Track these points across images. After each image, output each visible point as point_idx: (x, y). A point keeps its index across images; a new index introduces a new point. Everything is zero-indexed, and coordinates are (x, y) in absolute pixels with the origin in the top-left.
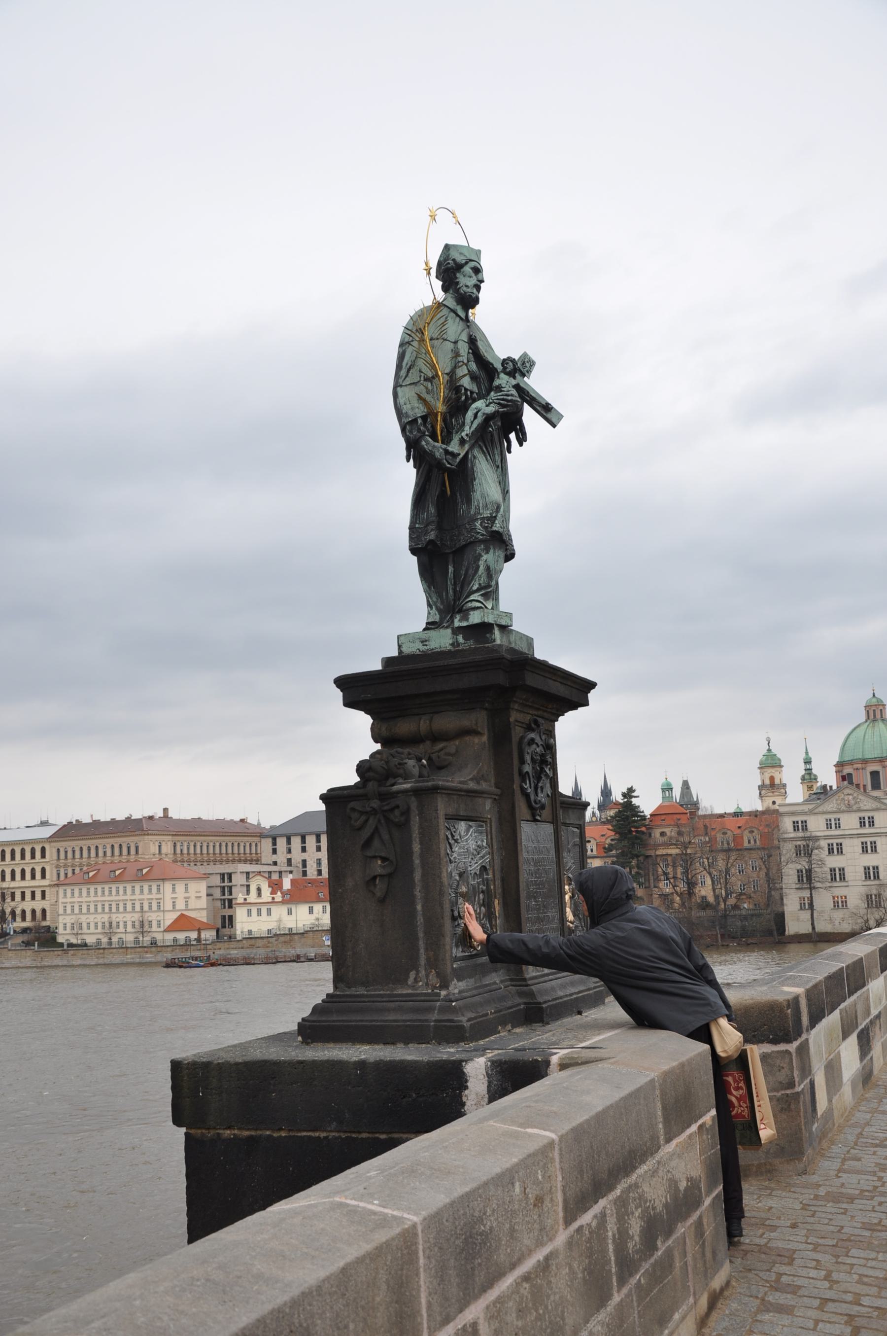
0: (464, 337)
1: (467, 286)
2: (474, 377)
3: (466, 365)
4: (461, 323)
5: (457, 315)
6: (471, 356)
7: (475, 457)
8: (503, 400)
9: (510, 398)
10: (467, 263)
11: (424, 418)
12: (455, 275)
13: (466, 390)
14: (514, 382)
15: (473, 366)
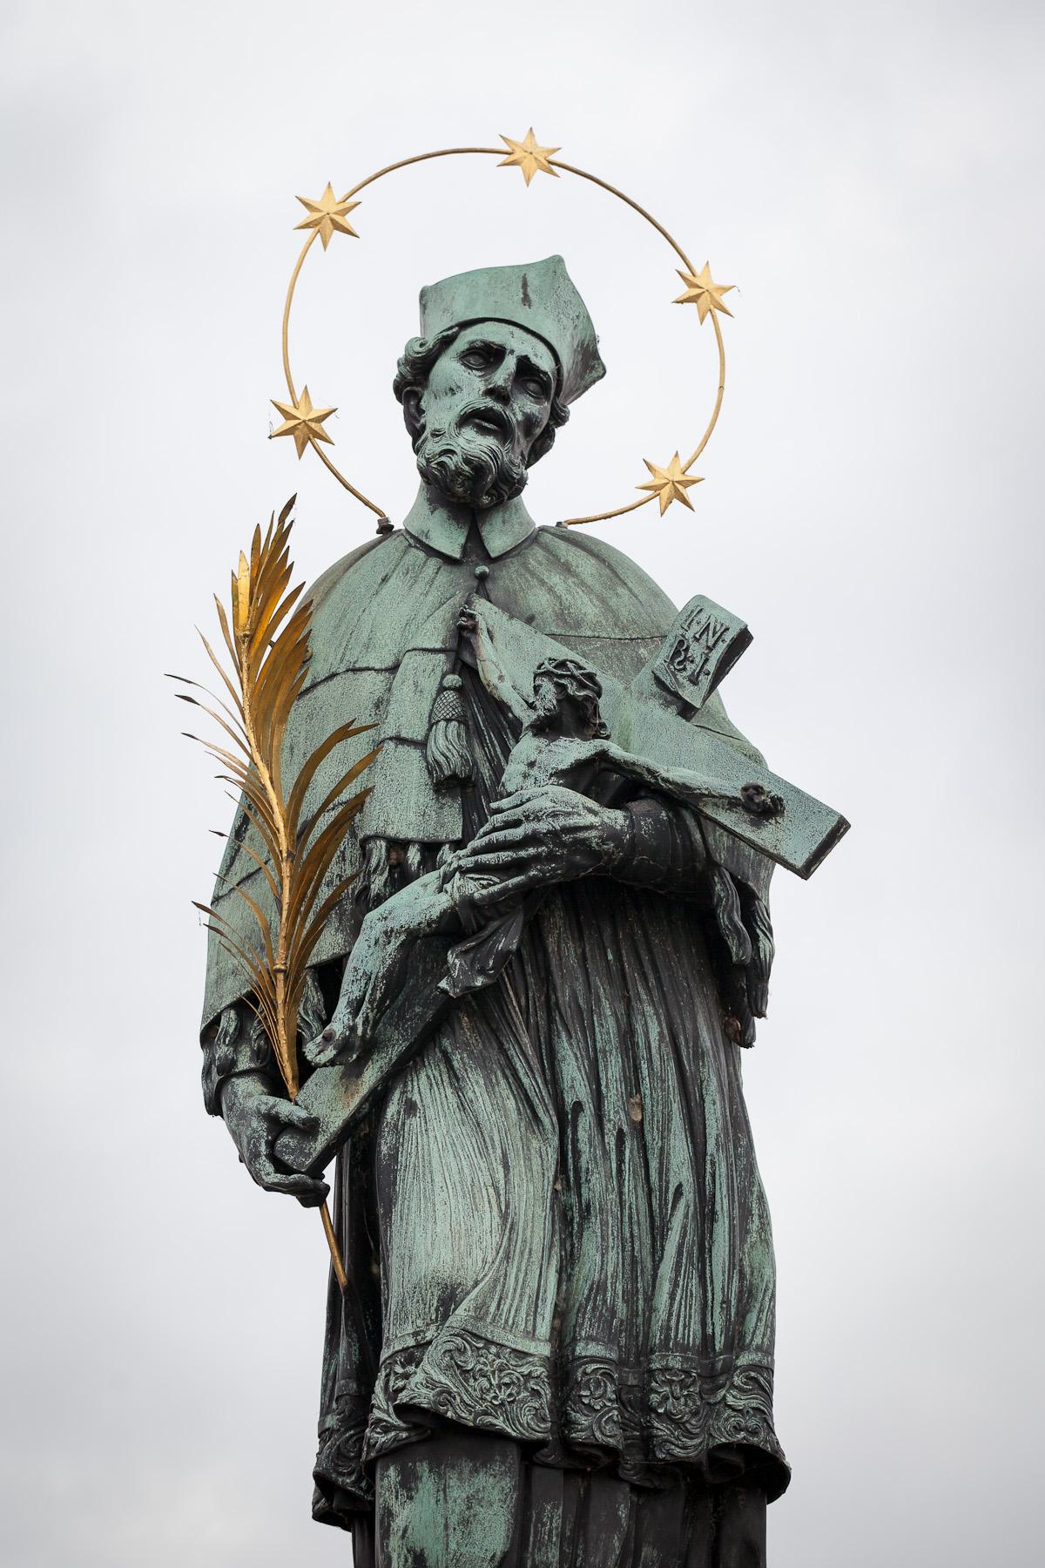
0: (434, 634)
1: (436, 434)
2: (448, 785)
3: (422, 745)
4: (445, 576)
5: (431, 552)
6: (450, 696)
7: (411, 1108)
9: (517, 833)
11: (244, 1007)
13: (398, 845)
15: (447, 743)
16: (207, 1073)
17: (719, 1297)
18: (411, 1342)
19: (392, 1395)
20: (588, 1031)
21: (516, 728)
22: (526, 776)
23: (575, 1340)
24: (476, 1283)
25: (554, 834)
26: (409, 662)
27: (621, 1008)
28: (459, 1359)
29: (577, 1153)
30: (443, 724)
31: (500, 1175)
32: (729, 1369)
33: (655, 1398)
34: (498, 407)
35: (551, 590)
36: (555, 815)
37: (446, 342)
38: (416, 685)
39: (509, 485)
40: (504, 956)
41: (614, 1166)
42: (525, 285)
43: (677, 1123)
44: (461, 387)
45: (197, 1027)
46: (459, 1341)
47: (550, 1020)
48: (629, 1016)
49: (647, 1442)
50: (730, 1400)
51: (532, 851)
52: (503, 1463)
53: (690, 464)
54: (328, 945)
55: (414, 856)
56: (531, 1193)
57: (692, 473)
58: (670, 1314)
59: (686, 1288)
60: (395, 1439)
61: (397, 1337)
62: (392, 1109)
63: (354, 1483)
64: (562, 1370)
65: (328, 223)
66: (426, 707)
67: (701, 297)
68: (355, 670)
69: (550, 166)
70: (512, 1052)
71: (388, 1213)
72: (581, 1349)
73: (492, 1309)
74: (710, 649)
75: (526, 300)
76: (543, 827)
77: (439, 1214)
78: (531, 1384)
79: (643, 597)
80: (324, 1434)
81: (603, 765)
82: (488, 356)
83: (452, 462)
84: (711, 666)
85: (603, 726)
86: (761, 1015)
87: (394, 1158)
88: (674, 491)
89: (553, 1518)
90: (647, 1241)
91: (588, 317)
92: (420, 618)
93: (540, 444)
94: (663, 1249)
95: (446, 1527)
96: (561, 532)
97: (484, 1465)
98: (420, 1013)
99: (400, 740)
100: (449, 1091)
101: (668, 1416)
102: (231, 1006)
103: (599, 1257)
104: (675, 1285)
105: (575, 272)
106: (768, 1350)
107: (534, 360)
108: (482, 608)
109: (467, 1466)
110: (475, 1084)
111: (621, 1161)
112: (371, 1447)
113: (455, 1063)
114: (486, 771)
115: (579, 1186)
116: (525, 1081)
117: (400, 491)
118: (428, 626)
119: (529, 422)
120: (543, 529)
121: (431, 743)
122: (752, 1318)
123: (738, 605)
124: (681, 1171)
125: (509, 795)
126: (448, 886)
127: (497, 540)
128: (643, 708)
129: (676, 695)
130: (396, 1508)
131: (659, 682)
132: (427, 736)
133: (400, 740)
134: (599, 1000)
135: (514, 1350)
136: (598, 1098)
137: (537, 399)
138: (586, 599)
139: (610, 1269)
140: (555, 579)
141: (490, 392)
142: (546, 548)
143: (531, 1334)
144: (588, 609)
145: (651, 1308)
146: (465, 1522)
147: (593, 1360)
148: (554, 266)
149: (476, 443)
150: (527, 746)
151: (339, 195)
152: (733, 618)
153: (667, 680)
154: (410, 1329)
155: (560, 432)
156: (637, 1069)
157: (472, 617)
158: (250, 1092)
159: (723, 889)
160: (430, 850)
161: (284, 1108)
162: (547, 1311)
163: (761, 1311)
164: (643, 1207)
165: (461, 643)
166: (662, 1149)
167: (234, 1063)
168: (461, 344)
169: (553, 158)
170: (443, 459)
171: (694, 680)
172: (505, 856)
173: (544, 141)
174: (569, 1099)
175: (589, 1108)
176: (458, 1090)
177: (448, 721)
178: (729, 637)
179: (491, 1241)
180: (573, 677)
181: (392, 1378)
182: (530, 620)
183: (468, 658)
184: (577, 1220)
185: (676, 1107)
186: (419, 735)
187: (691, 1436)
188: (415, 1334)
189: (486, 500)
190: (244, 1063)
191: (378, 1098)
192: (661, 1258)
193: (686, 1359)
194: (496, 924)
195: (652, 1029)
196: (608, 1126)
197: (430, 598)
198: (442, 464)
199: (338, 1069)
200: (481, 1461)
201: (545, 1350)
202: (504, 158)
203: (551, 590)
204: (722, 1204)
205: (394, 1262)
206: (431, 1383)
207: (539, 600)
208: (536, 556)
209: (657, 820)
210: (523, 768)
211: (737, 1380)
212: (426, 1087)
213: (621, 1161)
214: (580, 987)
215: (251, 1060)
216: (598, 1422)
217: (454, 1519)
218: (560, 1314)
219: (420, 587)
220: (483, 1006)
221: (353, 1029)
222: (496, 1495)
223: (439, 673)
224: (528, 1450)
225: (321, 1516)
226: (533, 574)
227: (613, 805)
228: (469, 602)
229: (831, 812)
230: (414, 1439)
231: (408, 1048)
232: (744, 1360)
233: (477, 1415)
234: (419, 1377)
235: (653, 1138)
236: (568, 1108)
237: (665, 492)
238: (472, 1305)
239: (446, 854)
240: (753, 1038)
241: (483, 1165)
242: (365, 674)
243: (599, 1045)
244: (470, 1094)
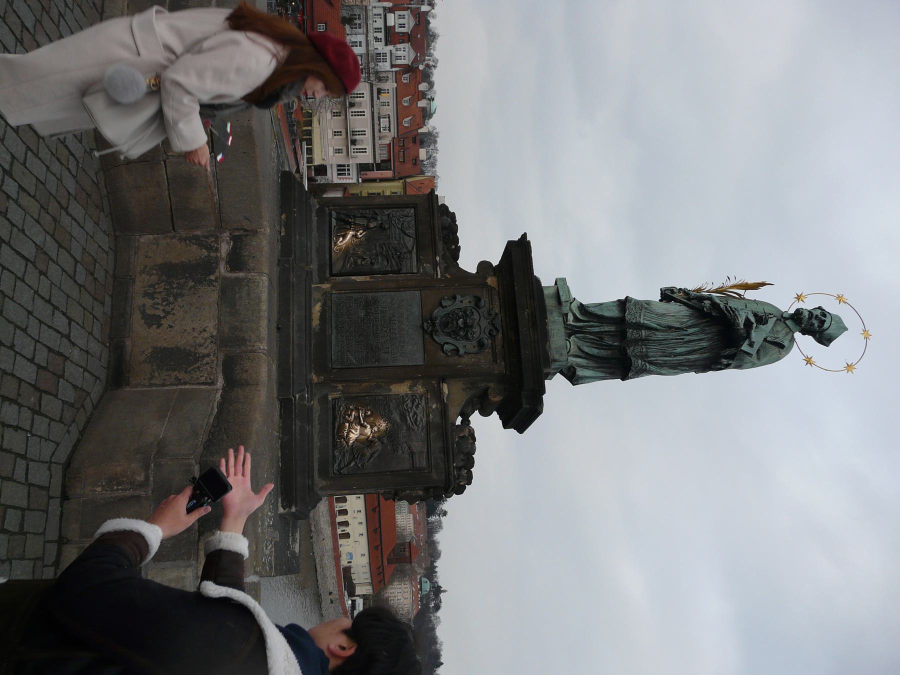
14: (753, 319)
40: (711, 313)
49: (629, 347)
64: (639, 326)
65: (840, 298)
67: (849, 367)
69: (866, 338)
82: (825, 316)
88: (809, 361)
89: (613, 329)
103: (660, 335)
106: (650, 372)
108: (775, 319)
119: (813, 325)
124: (679, 350)
127: (789, 322)
136: (689, 335)
140: (784, 332)
149: (806, 314)
159: (733, 350)
195: (704, 344)
200: (620, 311)
207: (779, 328)
216: (631, 333)
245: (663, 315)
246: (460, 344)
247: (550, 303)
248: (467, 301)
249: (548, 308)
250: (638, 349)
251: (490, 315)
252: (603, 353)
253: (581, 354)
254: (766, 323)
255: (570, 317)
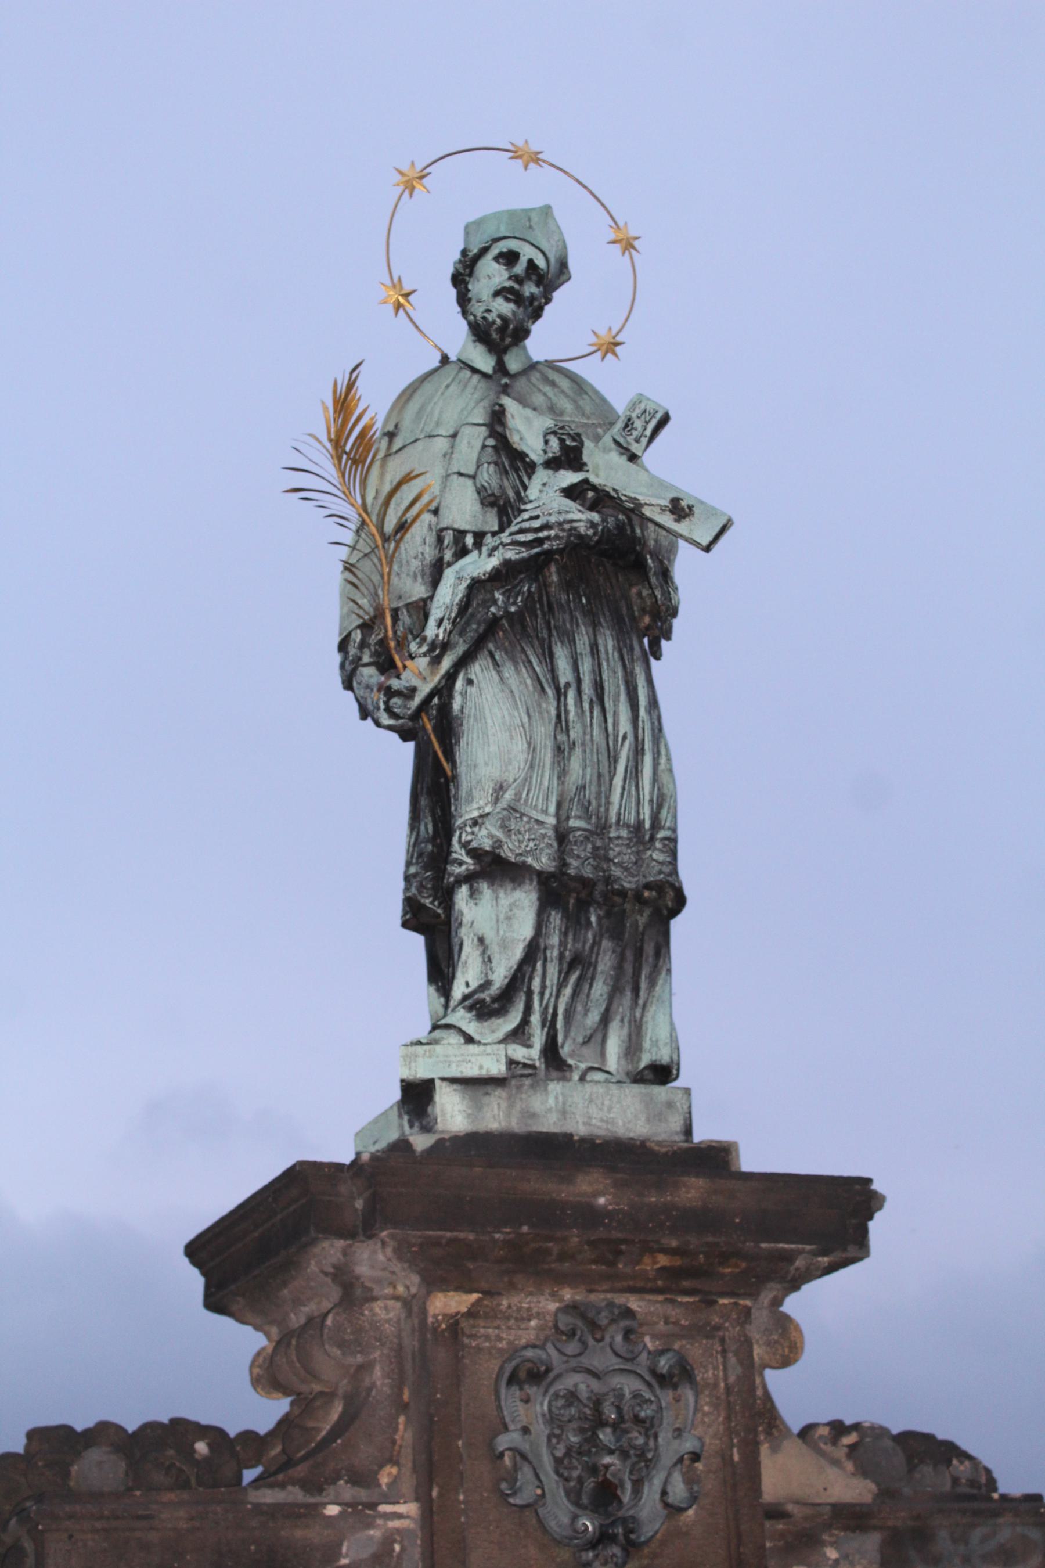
0: (480, 416)
2: (489, 500)
3: (473, 477)
4: (483, 384)
5: (475, 371)
6: (490, 450)
7: (470, 682)
8: (521, 531)
10: (484, 251)
11: (366, 627)
12: (467, 284)
13: (460, 534)
15: (489, 476)
16: (342, 666)
17: (647, 797)
18: (475, 814)
19: (465, 845)
20: (572, 642)
21: (531, 468)
22: (541, 491)
23: (568, 818)
24: (515, 780)
25: (560, 524)
26: (467, 432)
27: (591, 630)
28: (507, 823)
29: (567, 712)
30: (486, 465)
31: (526, 720)
32: (652, 838)
33: (611, 854)
34: (516, 286)
35: (545, 394)
36: (560, 513)
37: (484, 251)
38: (469, 443)
39: (521, 334)
41: (588, 719)
42: (529, 220)
43: (623, 697)
44: (491, 275)
45: (336, 640)
46: (505, 813)
47: (550, 636)
48: (595, 636)
50: (655, 856)
51: (545, 533)
52: (531, 884)
53: (618, 333)
54: (418, 591)
55: (469, 540)
56: (543, 732)
57: (619, 339)
58: (621, 806)
59: (629, 792)
60: (467, 870)
61: (467, 812)
62: (459, 684)
63: (432, 903)
64: (562, 836)
66: (475, 456)
68: (430, 436)
69: (535, 158)
70: (529, 652)
71: (458, 742)
72: (573, 823)
73: (524, 795)
74: (647, 423)
75: (531, 227)
76: (553, 519)
77: (491, 741)
78: (546, 840)
79: (597, 401)
80: (407, 878)
81: (586, 486)
82: (510, 258)
83: (490, 317)
84: (648, 433)
85: (585, 464)
86: (668, 638)
87: (462, 711)
88: (610, 347)
90: (606, 764)
91: (564, 242)
92: (469, 408)
93: (537, 314)
94: (615, 768)
95: (498, 921)
96: (550, 364)
97: (519, 885)
98: (474, 629)
99: (461, 474)
100: (494, 673)
101: (620, 865)
102: (359, 627)
104: (624, 789)
105: (557, 213)
106: (674, 830)
107: (536, 262)
109: (509, 886)
110: (508, 671)
111: (592, 717)
112: (450, 875)
113: (497, 657)
114: (511, 494)
115: (568, 731)
116: (537, 669)
117: (455, 336)
118: (475, 411)
119: (533, 298)
120: (537, 363)
121: (479, 478)
122: (664, 812)
123: (663, 399)
124: (625, 726)
125: (531, 501)
126: (496, 553)
127: (513, 364)
128: (606, 457)
129: (627, 449)
130: (465, 910)
131: (617, 443)
132: (476, 473)
133: (461, 474)
134: (578, 625)
135: (538, 822)
136: (579, 681)
137: (538, 286)
138: (566, 400)
139: (588, 777)
140: (547, 389)
141: (510, 278)
142: (540, 372)
143: (545, 812)
144: (567, 405)
145: (608, 803)
146: (508, 918)
147: (579, 829)
148: (546, 211)
149: (504, 307)
150: (542, 475)
151: (419, 167)
152: (659, 406)
153: (621, 441)
154: (475, 806)
155: (547, 308)
156: (600, 665)
157: (501, 406)
158: (369, 674)
160: (479, 537)
161: (395, 684)
162: (554, 800)
163: (669, 808)
164: (604, 745)
165: (497, 418)
166: (615, 712)
167: (360, 659)
168: (495, 251)
169: (540, 156)
170: (486, 315)
171: (637, 441)
172: (530, 537)
173: (534, 147)
174: (562, 681)
175: (574, 686)
176: (499, 673)
177: (489, 463)
178: (658, 416)
179: (522, 757)
180: (569, 434)
181: (464, 835)
182: (535, 409)
183: (499, 429)
184: (567, 749)
185: (622, 688)
186: (471, 472)
187: (633, 876)
188: (479, 808)
189: (508, 340)
190: (366, 659)
191: (451, 677)
192: (615, 774)
193: (630, 832)
194: (522, 576)
195: (608, 642)
196: (585, 697)
197: (475, 396)
198: (484, 318)
199: (427, 659)
201: (552, 821)
202: (511, 154)
203: (545, 394)
204: (648, 745)
205: (462, 769)
206: (491, 836)
207: (538, 400)
208: (535, 377)
209: (617, 519)
210: (539, 487)
211: (658, 845)
212: (478, 670)
213: (592, 717)
214: (567, 617)
215: (371, 657)
217: (502, 917)
218: (559, 805)
219: (469, 390)
220: (518, 621)
221: (437, 636)
222: (526, 903)
223: (482, 437)
224: (544, 879)
225: (405, 925)
226: (534, 386)
227: (592, 508)
228: (498, 397)
229: (723, 514)
230: (478, 868)
231: (469, 648)
232: (661, 834)
233: (517, 855)
234: (484, 832)
235: (608, 704)
236: (562, 685)
237: (604, 348)
238: (513, 792)
239: (489, 537)
240: (661, 655)
241: (516, 714)
242: (437, 439)
243: (578, 651)
244: (507, 675)
245: (531, 747)
246: (670, 1447)
247: (497, 1115)
248: (521, 1408)
249: (515, 1125)
250: (621, 853)
251: (572, 1334)
252: (605, 963)
253: (599, 1036)
254: (577, 437)
255: (519, 1052)
